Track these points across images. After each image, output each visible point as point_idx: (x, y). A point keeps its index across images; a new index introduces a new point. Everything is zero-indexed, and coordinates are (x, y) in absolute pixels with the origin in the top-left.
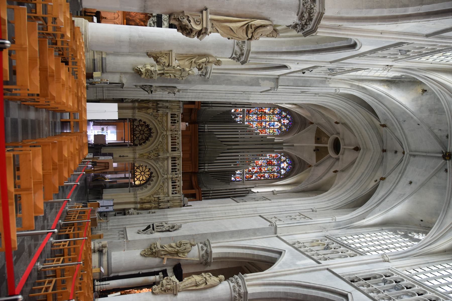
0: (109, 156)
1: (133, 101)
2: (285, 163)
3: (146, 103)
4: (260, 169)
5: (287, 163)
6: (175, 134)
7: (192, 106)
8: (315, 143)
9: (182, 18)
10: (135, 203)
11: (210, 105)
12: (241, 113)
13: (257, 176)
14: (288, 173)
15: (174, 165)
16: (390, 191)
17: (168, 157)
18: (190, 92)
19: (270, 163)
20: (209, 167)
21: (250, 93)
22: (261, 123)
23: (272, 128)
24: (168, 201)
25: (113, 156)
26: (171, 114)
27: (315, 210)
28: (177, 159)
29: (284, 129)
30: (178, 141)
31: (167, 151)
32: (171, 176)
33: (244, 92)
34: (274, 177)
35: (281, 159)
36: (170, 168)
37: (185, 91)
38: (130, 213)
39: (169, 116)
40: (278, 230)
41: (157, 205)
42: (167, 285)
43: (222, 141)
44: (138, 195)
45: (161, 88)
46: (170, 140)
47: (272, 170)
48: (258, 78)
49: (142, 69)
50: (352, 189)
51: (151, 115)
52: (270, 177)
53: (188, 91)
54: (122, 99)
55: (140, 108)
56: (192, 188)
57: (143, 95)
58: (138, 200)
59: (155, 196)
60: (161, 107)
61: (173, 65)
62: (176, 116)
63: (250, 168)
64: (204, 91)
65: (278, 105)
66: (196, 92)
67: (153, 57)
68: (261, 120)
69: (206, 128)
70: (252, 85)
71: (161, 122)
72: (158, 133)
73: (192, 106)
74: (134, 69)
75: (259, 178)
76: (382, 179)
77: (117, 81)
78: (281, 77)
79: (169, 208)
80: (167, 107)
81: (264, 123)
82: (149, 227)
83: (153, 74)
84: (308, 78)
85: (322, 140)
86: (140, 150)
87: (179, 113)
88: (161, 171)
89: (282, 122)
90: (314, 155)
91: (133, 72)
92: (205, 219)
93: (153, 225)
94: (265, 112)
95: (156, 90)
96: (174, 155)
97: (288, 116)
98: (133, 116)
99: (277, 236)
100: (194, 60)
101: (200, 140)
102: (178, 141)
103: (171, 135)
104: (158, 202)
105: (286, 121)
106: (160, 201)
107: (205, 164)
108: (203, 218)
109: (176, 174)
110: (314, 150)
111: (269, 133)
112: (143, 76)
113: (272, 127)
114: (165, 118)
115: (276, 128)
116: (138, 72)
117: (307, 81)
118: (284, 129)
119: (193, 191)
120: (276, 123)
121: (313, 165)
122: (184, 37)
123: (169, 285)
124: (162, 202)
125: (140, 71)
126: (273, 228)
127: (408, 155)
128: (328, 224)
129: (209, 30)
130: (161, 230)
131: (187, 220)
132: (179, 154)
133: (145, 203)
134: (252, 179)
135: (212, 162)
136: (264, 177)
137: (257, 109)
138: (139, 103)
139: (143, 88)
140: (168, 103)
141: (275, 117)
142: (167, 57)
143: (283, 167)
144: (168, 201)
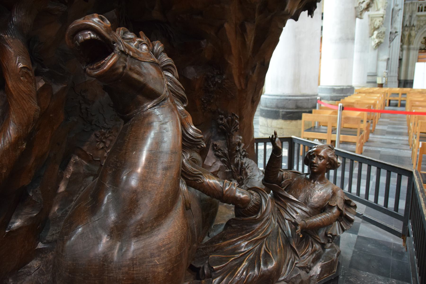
1: (402, 50)
3: (404, 38)
26: (419, 11)
39: (420, 13)
45: (393, 23)
49: (375, 42)
51: (418, 32)
55: (409, 43)
57: (397, 40)
60: (410, 23)
62: (420, 7)
74: (375, 49)
77: (385, 64)
80: (411, 16)
83: (381, 32)
91: (377, 51)
95: (395, 28)
112: (382, 40)
114: (422, 18)
116: (379, 45)
125: (377, 43)
139: (391, 40)
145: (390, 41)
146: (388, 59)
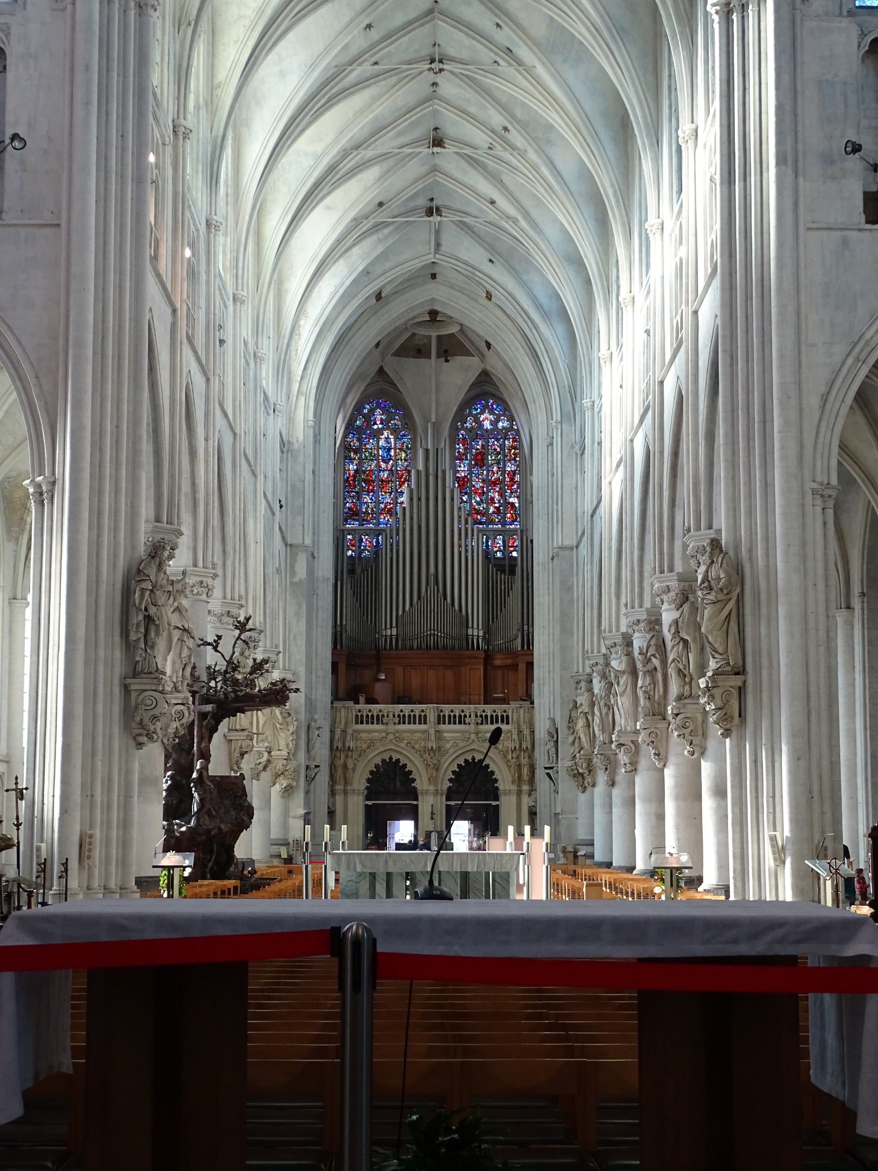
0: (430, 838)
1: (333, 793)
2: (482, 417)
3: (336, 771)
4: (494, 483)
5: (482, 412)
6: (394, 716)
7: (342, 667)
8: (430, 358)
10: (519, 793)
11: (339, 629)
12: (357, 538)
13: (512, 493)
14: (506, 410)
15: (452, 720)
16: (509, 297)
17: (436, 731)
19: (479, 457)
20: (475, 626)
22: (382, 481)
23: (395, 452)
24: (520, 732)
25: (432, 832)
26: (357, 723)
27: (549, 440)
28: (442, 714)
29: (396, 422)
30: (407, 712)
31: (425, 731)
32: (472, 726)
34: (515, 448)
35: (472, 428)
36: (458, 727)
38: (533, 804)
40: (567, 542)
41: (526, 754)
42: (582, 767)
43: (419, 598)
44: (507, 788)
46: (406, 727)
47: (499, 453)
48: (292, 583)
50: (513, 348)
52: (514, 459)
54: (329, 813)
56: (518, 665)
58: (514, 788)
59: (510, 757)
61: (287, 754)
62: (359, 714)
63: (492, 509)
65: (337, 446)
67: (276, 778)
68: (373, 482)
69: (389, 633)
71: (371, 744)
72: (390, 749)
73: (342, 667)
75: (515, 486)
76: (489, 297)
78: (289, 542)
79: (533, 732)
81: (382, 474)
82: (549, 775)
84: (289, 487)
85: (420, 342)
86: (421, 783)
87: (352, 708)
88: (462, 744)
89: (380, 426)
90: (458, 361)
92: (551, 669)
93: (546, 768)
94: (356, 471)
95: (314, 760)
96: (432, 720)
97: (366, 411)
98: (358, 795)
99: (577, 547)
100: (278, 726)
101: (415, 647)
102: (407, 712)
103: (395, 724)
104: (520, 751)
105: (379, 415)
106: (517, 748)
107: (467, 635)
108: (549, 672)
109: (470, 716)
110: (447, 361)
111: (405, 460)
112: (295, 784)
113: (392, 453)
114: (363, 735)
115: (395, 444)
117: (293, 486)
118: (396, 422)
119: (522, 667)
120: (382, 443)
121: (482, 366)
123: (582, 765)
124: (521, 744)
125: (285, 788)
126: (562, 553)
127: (437, 256)
128: (565, 438)
129: (266, 744)
130: (554, 755)
131: (549, 702)
132: (430, 710)
133: (520, 776)
134: (517, 505)
135: (465, 619)
136: (514, 473)
137: (348, 492)
138: (336, 783)
140: (336, 730)
141: (368, 446)
142: (276, 762)
143: (492, 423)
144: (520, 732)
146: (307, 814)
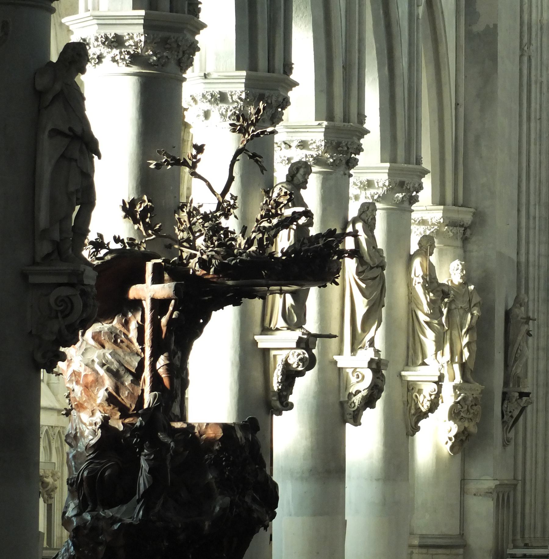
9: (353, 405)
18: (528, 253)
21: (525, 28)
33: (521, 49)
37: (523, 269)
48: (470, 36)
53: (523, 259)
64: (524, 200)
66: (528, 229)
70: (494, 58)
95: (518, 381)
112: (473, 429)
122: (383, 394)
145: (504, 423)
